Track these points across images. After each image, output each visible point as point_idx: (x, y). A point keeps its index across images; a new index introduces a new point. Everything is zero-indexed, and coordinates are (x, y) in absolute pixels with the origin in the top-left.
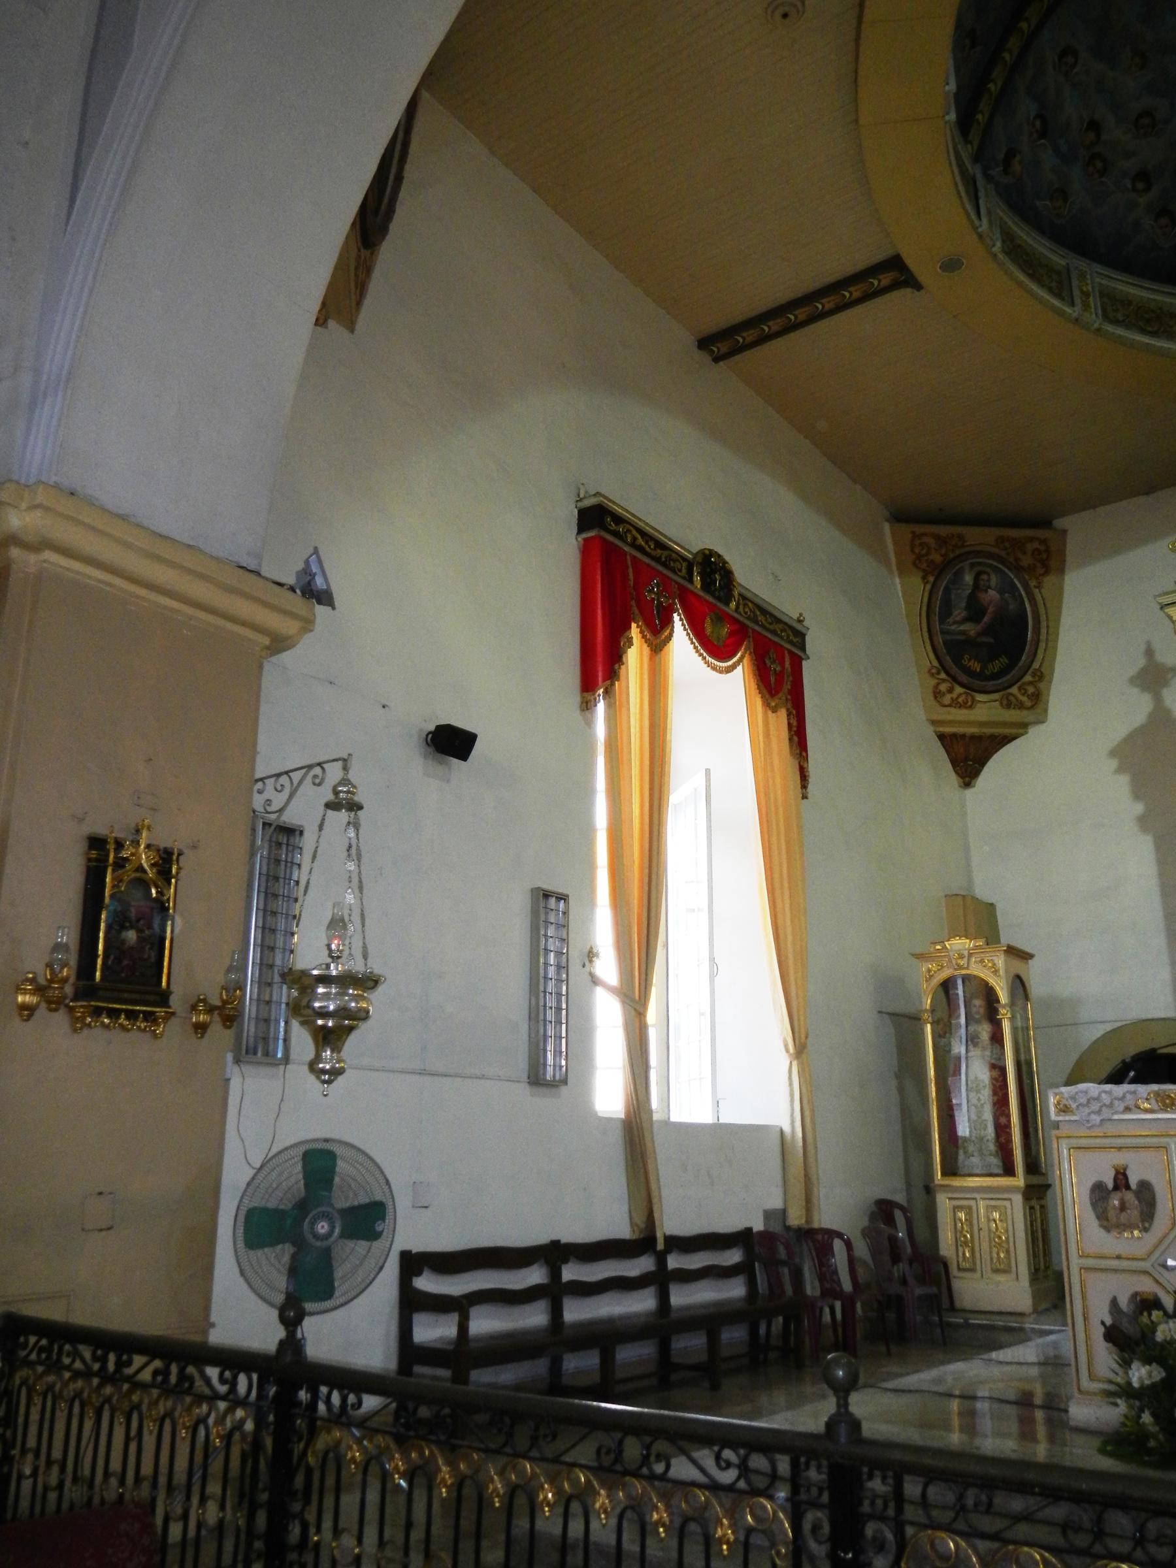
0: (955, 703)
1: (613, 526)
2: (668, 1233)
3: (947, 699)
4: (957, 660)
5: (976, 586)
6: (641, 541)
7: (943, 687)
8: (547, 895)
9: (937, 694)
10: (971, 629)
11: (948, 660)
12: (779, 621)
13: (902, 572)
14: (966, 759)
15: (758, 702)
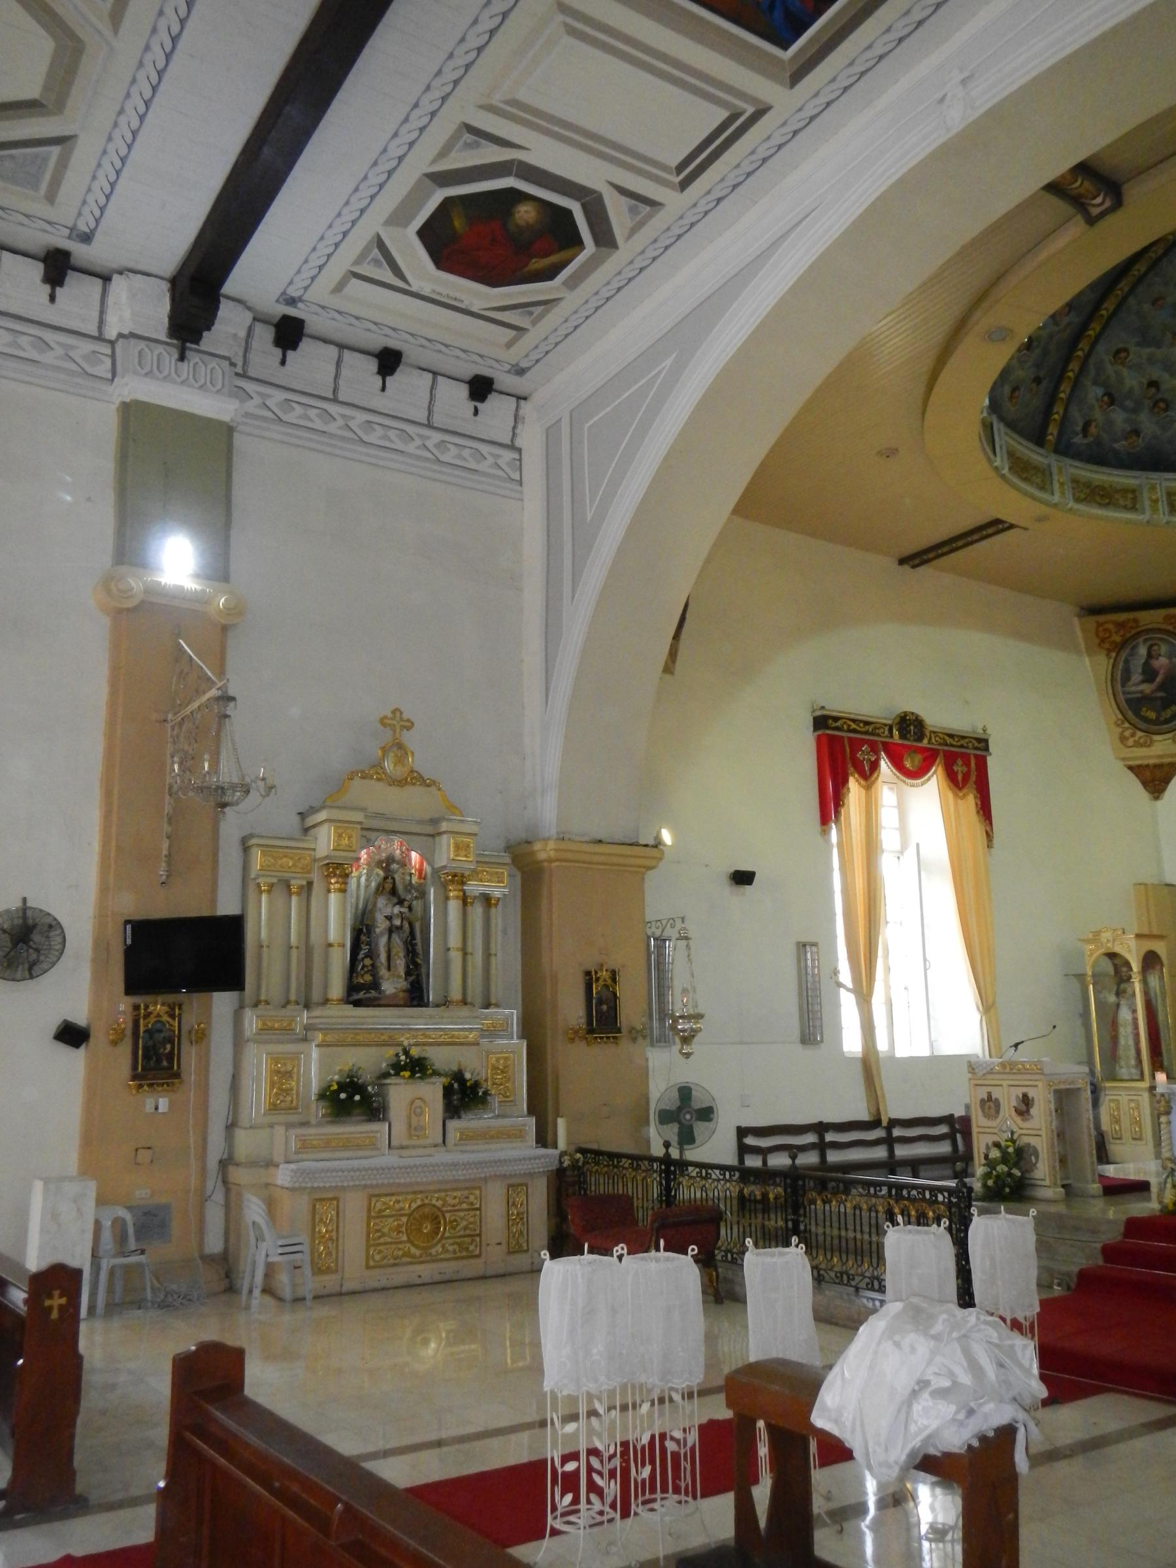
0: (1137, 744)
1: (834, 725)
2: (893, 1117)
3: (1131, 742)
4: (1137, 713)
5: (1150, 655)
6: (853, 726)
7: (1127, 734)
8: (804, 946)
9: (1123, 739)
10: (1147, 688)
11: (1130, 714)
12: (963, 737)
13: (1090, 652)
14: (1153, 780)
15: (950, 795)
